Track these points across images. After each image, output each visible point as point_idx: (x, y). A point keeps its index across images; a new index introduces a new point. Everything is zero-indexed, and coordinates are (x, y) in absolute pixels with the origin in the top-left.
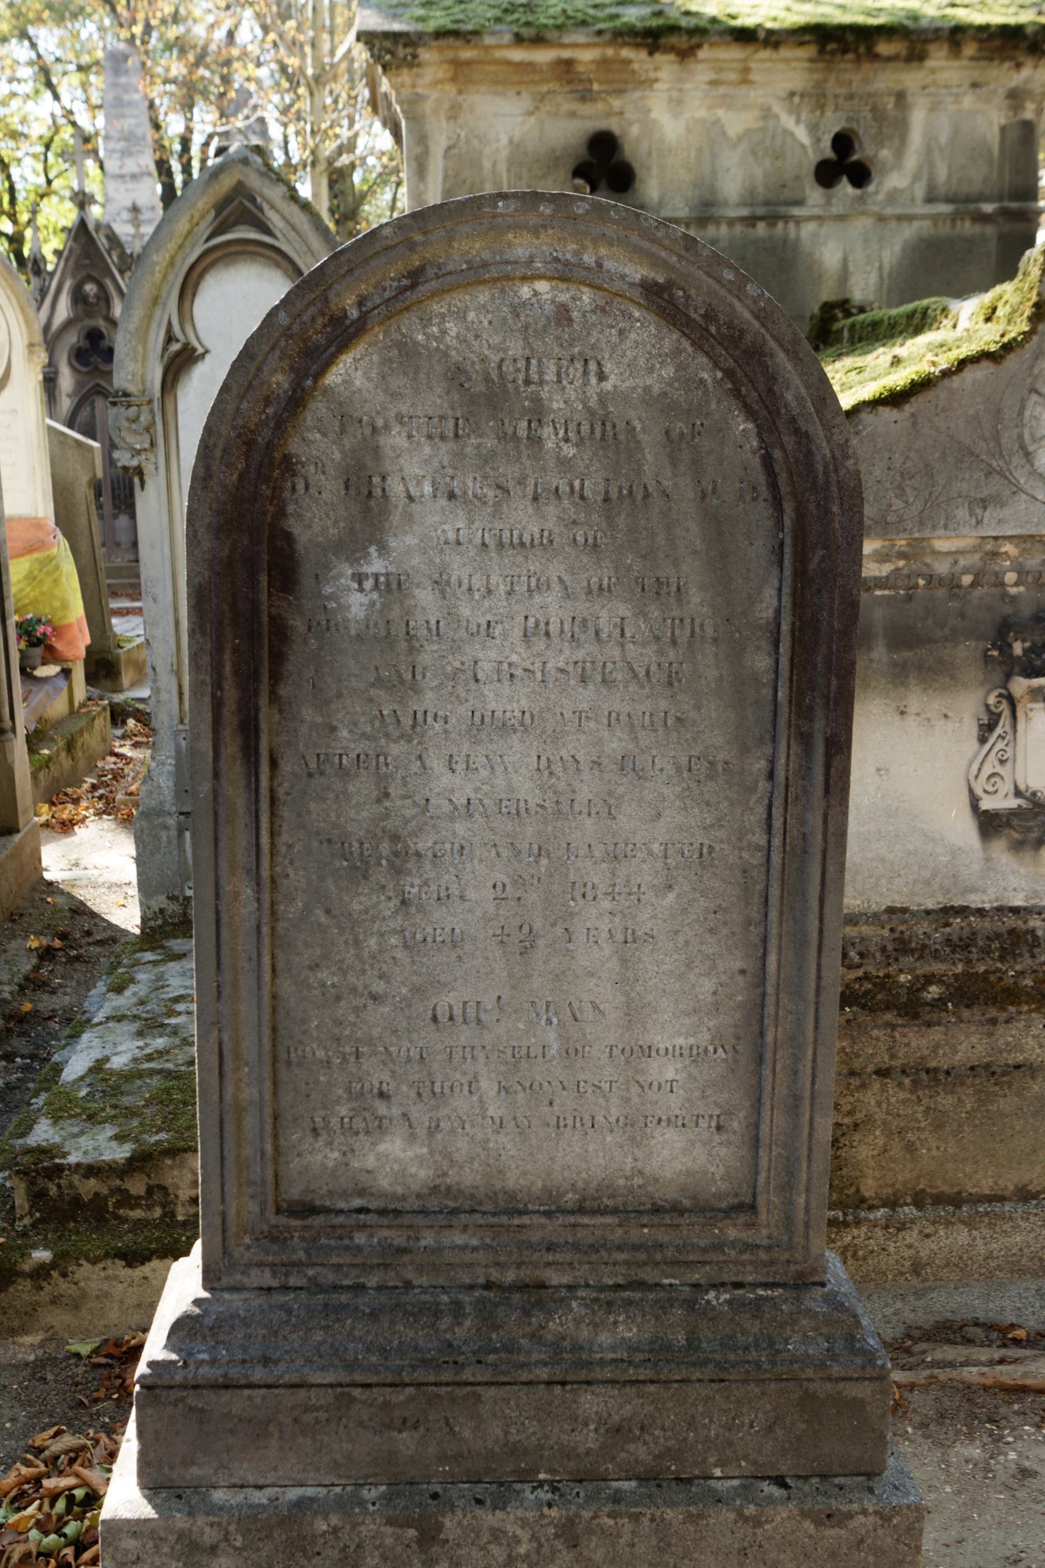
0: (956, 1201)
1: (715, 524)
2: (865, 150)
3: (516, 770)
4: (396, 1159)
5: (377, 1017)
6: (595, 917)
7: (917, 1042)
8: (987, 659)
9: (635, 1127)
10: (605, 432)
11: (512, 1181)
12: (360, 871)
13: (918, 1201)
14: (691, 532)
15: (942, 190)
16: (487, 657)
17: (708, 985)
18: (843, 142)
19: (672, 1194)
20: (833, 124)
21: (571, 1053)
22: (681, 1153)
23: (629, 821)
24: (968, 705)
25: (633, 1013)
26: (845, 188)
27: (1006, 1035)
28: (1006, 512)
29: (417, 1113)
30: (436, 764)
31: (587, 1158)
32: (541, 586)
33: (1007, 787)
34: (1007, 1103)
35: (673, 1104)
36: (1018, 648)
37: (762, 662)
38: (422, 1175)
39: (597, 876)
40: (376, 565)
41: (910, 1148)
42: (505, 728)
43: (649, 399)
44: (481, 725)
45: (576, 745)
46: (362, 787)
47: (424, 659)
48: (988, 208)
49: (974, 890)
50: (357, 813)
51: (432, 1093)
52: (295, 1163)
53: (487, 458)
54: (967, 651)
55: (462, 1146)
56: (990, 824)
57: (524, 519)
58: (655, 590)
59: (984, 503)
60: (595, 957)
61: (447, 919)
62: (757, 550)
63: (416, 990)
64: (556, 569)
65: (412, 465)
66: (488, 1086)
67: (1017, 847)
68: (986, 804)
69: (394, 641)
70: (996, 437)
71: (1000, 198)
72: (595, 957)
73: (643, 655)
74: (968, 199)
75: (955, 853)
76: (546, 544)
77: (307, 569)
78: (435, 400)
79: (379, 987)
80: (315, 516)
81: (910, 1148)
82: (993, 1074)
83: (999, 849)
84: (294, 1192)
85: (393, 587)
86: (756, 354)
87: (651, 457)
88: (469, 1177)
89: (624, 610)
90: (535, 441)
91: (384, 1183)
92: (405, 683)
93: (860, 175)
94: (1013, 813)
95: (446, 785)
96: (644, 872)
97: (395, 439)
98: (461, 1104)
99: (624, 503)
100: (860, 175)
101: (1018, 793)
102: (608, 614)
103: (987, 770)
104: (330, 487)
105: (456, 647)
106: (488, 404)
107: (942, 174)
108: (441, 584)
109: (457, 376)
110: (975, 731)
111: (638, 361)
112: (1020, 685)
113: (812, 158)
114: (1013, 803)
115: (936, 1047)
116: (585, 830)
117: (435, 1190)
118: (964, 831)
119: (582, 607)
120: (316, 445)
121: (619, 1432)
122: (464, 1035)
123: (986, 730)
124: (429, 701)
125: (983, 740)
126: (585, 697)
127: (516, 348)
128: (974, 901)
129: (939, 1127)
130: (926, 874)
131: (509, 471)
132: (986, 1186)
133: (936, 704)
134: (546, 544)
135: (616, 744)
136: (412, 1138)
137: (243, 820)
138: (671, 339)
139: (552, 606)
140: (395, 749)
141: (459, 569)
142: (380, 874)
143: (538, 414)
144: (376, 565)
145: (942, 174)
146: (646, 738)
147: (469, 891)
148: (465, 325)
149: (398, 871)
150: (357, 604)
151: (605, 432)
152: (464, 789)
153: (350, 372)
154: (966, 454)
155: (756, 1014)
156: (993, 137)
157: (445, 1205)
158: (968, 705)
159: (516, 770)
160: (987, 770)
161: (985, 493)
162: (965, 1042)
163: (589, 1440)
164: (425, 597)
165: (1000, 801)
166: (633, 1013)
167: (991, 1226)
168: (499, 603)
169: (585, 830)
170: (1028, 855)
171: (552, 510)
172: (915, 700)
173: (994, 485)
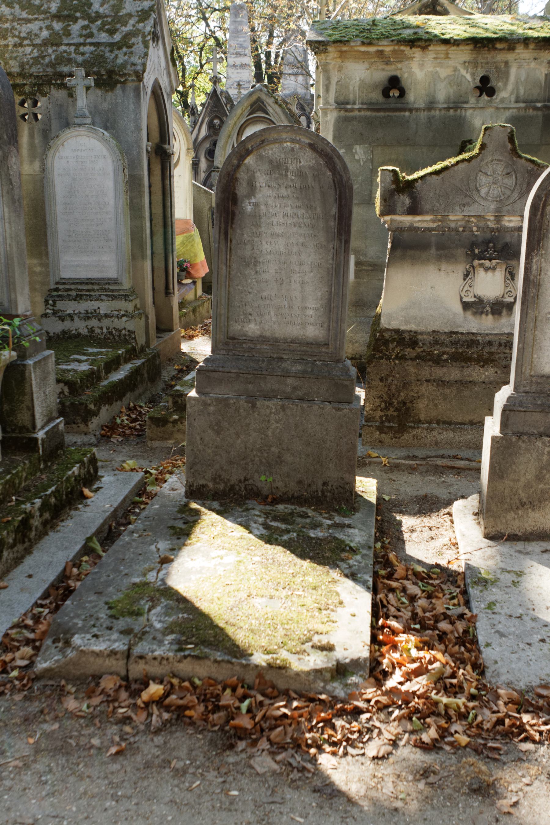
0: (450, 423)
2: (493, 83)
3: (280, 245)
4: (252, 329)
6: (296, 277)
7: (439, 372)
8: (467, 254)
9: (303, 325)
10: (301, 174)
11: (277, 335)
12: (248, 265)
13: (438, 422)
14: (318, 195)
15: (522, 98)
16: (275, 220)
17: (320, 294)
18: (485, 80)
19: (311, 341)
20: (481, 73)
21: (290, 307)
22: (313, 332)
24: (461, 269)
25: (303, 299)
26: (485, 97)
27: (467, 371)
28: (471, 208)
29: (257, 318)
30: (264, 243)
31: (293, 331)
33: (471, 295)
34: (467, 393)
35: (312, 320)
36: (477, 251)
37: (332, 224)
38: (258, 333)
39: (297, 268)
40: (253, 200)
41: (436, 405)
42: (278, 236)
43: (310, 168)
44: (274, 235)
45: (293, 240)
46: (249, 247)
47: (262, 220)
48: (539, 105)
49: (460, 327)
50: (247, 252)
51: (261, 315)
52: (232, 328)
53: (276, 179)
54: (460, 252)
55: (266, 327)
56: (466, 306)
57: (284, 192)
58: (310, 207)
59: (464, 205)
61: (265, 276)
63: (259, 292)
64: (290, 202)
65: (261, 180)
66: (272, 314)
67: (475, 314)
68: (465, 299)
69: (256, 216)
70: (468, 185)
71: (544, 101)
74: (532, 102)
75: (455, 314)
76: (288, 197)
77: (239, 201)
78: (266, 167)
79: (250, 290)
80: (241, 190)
81: (436, 405)
82: (463, 384)
83: (469, 314)
85: (256, 205)
86: (331, 158)
87: (310, 180)
88: (268, 334)
89: (303, 211)
90: (286, 175)
91: (250, 334)
92: (258, 225)
93: (491, 92)
94: (474, 303)
95: (266, 247)
96: (306, 268)
97: (258, 174)
98: (267, 317)
100: (491, 92)
101: (475, 297)
102: (300, 212)
103: (465, 289)
104: (244, 184)
105: (269, 218)
106: (277, 168)
107: (522, 92)
108: (266, 205)
109: (271, 162)
110: (462, 277)
112: (476, 262)
113: (472, 85)
114: (473, 299)
115: (444, 374)
117: (260, 336)
118: (458, 308)
119: (295, 210)
120: (242, 175)
121: (295, 388)
122: (268, 302)
123: (466, 276)
124: (263, 229)
125: (465, 280)
126: (295, 229)
127: (283, 156)
128: (460, 330)
129: (445, 399)
130: (445, 321)
131: (281, 182)
132: (460, 420)
133: (450, 268)
134: (288, 197)
135: (301, 240)
136: (256, 324)
137: (224, 253)
138: (314, 155)
139: (289, 210)
140: (256, 239)
141: (270, 202)
142: (251, 266)
143: (287, 170)
144: (253, 200)
145: (522, 92)
146: (307, 239)
147: (270, 270)
148: (272, 151)
149: (255, 265)
150: (249, 208)
151: (301, 174)
153: (249, 160)
155: (330, 300)
156: (542, 78)
157: (263, 339)
158: (461, 269)
159: (280, 245)
160: (465, 289)
161: (464, 202)
162: (454, 373)
163: (289, 389)
164: (263, 207)
165: (469, 299)
166: (303, 299)
167: (461, 432)
168: (278, 209)
169: (294, 258)
170: (478, 317)
171: (289, 190)
172: (444, 266)
173: (468, 200)
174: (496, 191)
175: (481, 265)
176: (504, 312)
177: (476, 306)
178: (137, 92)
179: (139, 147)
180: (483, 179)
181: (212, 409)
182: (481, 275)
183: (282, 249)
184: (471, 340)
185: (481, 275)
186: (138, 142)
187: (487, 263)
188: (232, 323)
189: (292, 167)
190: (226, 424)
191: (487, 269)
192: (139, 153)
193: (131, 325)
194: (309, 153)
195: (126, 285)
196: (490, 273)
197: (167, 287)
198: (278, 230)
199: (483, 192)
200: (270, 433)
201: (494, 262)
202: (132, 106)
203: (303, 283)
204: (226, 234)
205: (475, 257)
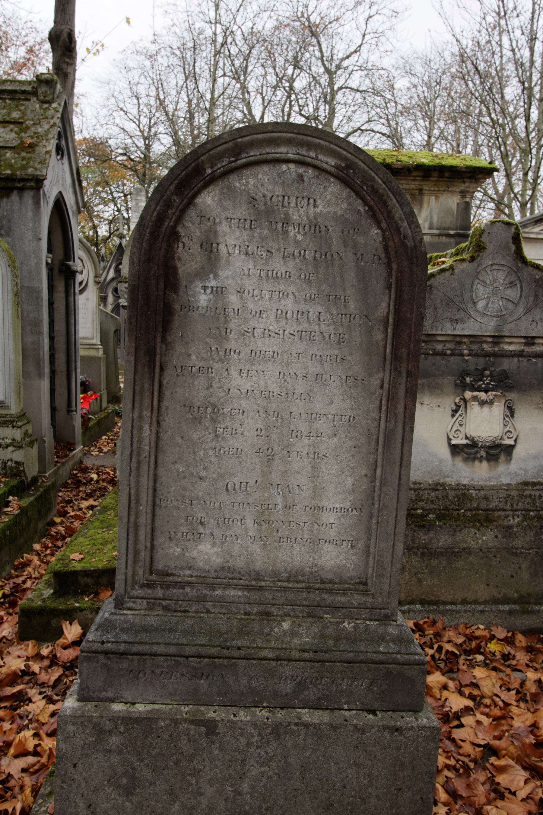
0: (436, 603)
1: (363, 275)
3: (269, 378)
4: (206, 553)
5: (201, 488)
6: (302, 445)
9: (315, 543)
10: (315, 228)
11: (258, 565)
12: (198, 420)
13: (423, 602)
14: (351, 275)
15: (435, 225)
16: (259, 327)
17: (350, 481)
19: (330, 576)
22: (335, 556)
23: (319, 405)
24: (449, 402)
27: (459, 536)
28: (466, 325)
29: (218, 533)
30: (234, 373)
31: (294, 556)
32: (284, 295)
33: (462, 435)
34: (460, 564)
35: (333, 534)
36: (468, 380)
37: (379, 336)
39: (304, 429)
41: (420, 581)
42: (265, 359)
43: (335, 217)
45: (296, 368)
46: (200, 382)
47: (232, 326)
48: (452, 232)
49: (448, 477)
52: (160, 552)
53: (264, 239)
54: (448, 381)
56: (455, 450)
57: (278, 265)
58: (333, 300)
59: (457, 321)
60: (301, 465)
63: (220, 476)
64: (292, 289)
65: (230, 238)
66: (249, 522)
67: (466, 460)
68: (454, 442)
69: (219, 316)
70: (462, 296)
71: (456, 229)
72: (301, 465)
74: (445, 229)
75: (441, 461)
76: (288, 276)
77: (183, 283)
79: (203, 473)
81: (420, 581)
84: (159, 565)
85: (219, 292)
86: (382, 201)
87: (336, 244)
88: (239, 564)
89: (320, 309)
90: (286, 233)
91: (200, 564)
92: (222, 336)
94: (467, 446)
95: (238, 382)
96: (324, 426)
97: (224, 228)
98: (237, 528)
99: (323, 262)
101: (467, 438)
102: (314, 309)
103: (455, 428)
104: (195, 248)
105: (245, 321)
106: (265, 216)
107: (435, 219)
108: (240, 292)
110: (450, 413)
112: (468, 394)
114: (464, 442)
115: (430, 541)
116: (298, 407)
117: (223, 568)
118: (445, 452)
119: (303, 307)
121: (301, 685)
122: (240, 497)
124: (233, 345)
125: (453, 416)
126: (301, 347)
127: (279, 191)
128: (448, 480)
129: (431, 573)
130: (429, 469)
131: (274, 245)
132: (450, 598)
133: (435, 401)
134: (288, 276)
135: (314, 368)
136: (214, 544)
137: (147, 393)
138: (346, 192)
139: (289, 305)
140: (216, 366)
141: (249, 285)
142: (206, 422)
143: (286, 222)
144: (213, 283)
145: (435, 219)
146: (328, 367)
147: (246, 431)
149: (214, 421)
150: (203, 299)
151: (315, 228)
156: (454, 207)
157: (226, 576)
158: (449, 402)
159: (269, 378)
160: (455, 428)
161: (457, 318)
163: (288, 687)
164: (233, 299)
166: (316, 492)
167: (451, 615)
168: (266, 303)
169: (298, 407)
170: (470, 464)
171: (291, 263)
173: (461, 314)
174: (496, 305)
175: (475, 398)
176: (502, 457)
177: (468, 450)
178: (37, 203)
179: (39, 258)
180: (481, 291)
181: (114, 740)
182: (475, 409)
183: (274, 387)
184: (463, 493)
185: (475, 409)
186: (37, 252)
187: (483, 396)
188: (160, 540)
189: (299, 213)
190: (147, 774)
191: (482, 403)
192: (38, 264)
193: (18, 456)
194: (334, 188)
195: (14, 409)
196: (486, 409)
197: (69, 405)
199: (481, 305)
200: (245, 787)
201: (491, 394)
202: (30, 214)
203: (317, 457)
204: (151, 353)
205: (463, 387)
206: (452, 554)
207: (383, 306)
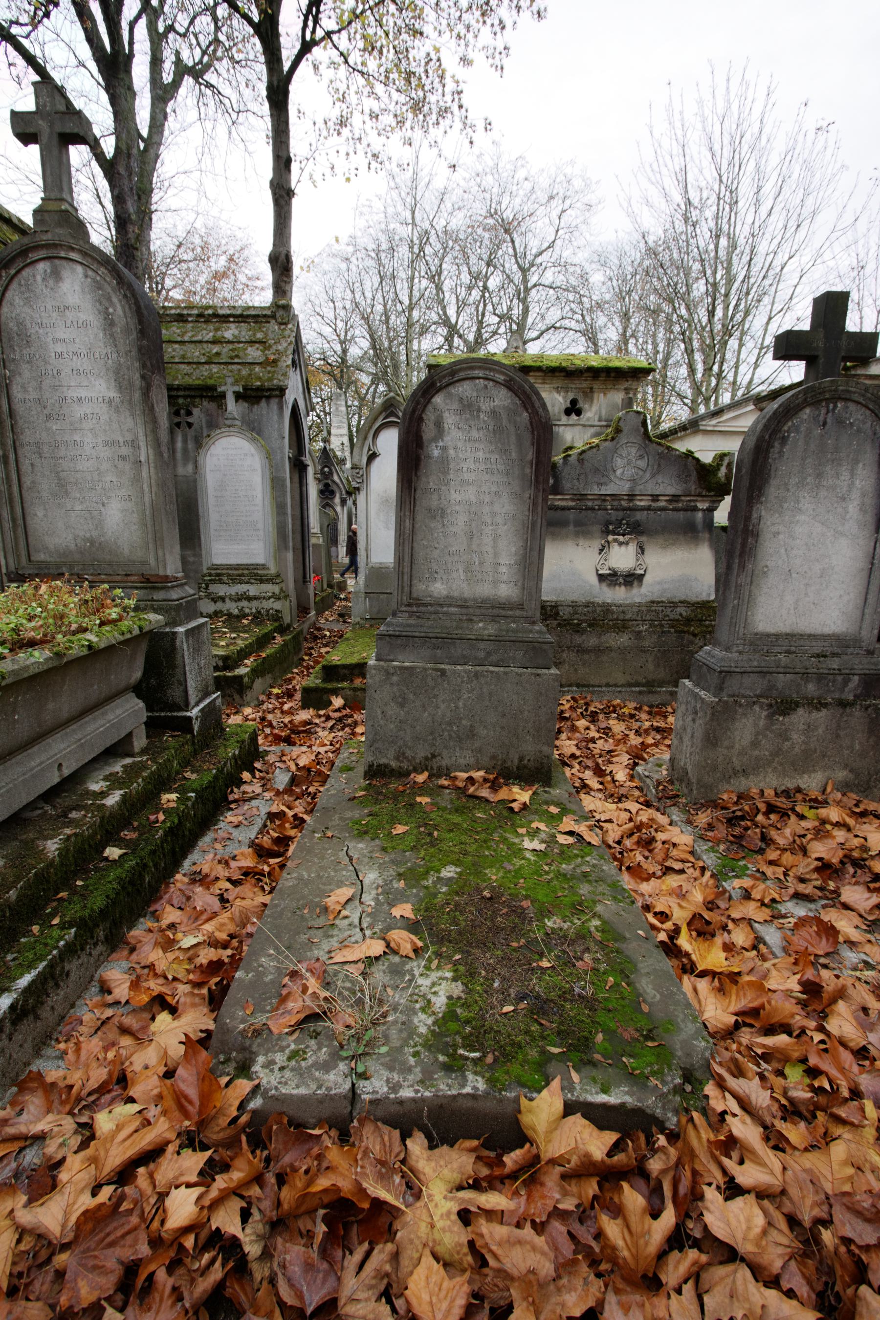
0: (588, 686)
1: (519, 438)
2: (580, 404)
3: (471, 494)
4: (439, 589)
5: (436, 553)
6: (488, 530)
7: (578, 639)
9: (495, 583)
10: (494, 413)
11: (466, 595)
13: (578, 686)
14: (513, 439)
16: (465, 466)
18: (574, 402)
20: (571, 396)
21: (481, 563)
23: (497, 508)
24: (597, 544)
25: (496, 555)
26: (574, 417)
31: (484, 590)
32: (478, 450)
34: (604, 658)
35: (505, 578)
37: (528, 471)
38: (445, 593)
39: (489, 521)
40: (441, 444)
42: (468, 484)
43: (504, 407)
44: (463, 482)
45: (485, 488)
46: (435, 497)
50: (434, 504)
51: (447, 571)
54: (597, 528)
55: (454, 587)
56: (602, 578)
57: (475, 434)
58: (504, 452)
60: (488, 540)
61: (453, 529)
62: (527, 443)
65: (450, 420)
67: (609, 585)
69: (444, 461)
72: (488, 540)
73: (501, 467)
76: (480, 439)
78: (456, 406)
80: (428, 430)
83: (604, 585)
84: (415, 595)
85: (444, 449)
86: (529, 398)
87: (505, 422)
88: (456, 594)
92: (446, 472)
93: (579, 413)
95: (454, 496)
96: (499, 519)
97: (446, 415)
98: (455, 575)
99: (498, 431)
100: (579, 413)
104: (431, 425)
106: (468, 407)
107: (604, 413)
109: (461, 399)
111: (502, 398)
112: (610, 538)
113: (564, 407)
116: (486, 509)
118: (594, 580)
120: (429, 416)
123: (601, 550)
124: (451, 476)
126: (487, 477)
128: (597, 600)
133: (587, 543)
134: (480, 439)
135: (494, 489)
138: (510, 394)
139: (481, 455)
141: (460, 445)
143: (479, 410)
144: (441, 444)
145: (604, 413)
147: (459, 522)
148: (465, 389)
150: (436, 453)
151: (494, 413)
152: (459, 498)
153: (438, 399)
154: (597, 470)
155: (524, 556)
156: (620, 402)
157: (449, 601)
158: (597, 544)
159: (471, 494)
162: (592, 641)
163: (482, 655)
164: (451, 452)
165: (605, 571)
166: (496, 555)
169: (486, 509)
172: (581, 542)
174: (630, 472)
175: (615, 540)
176: (636, 583)
177: (610, 578)
178: (281, 408)
179: (283, 452)
180: (619, 462)
181: (395, 679)
182: (615, 549)
183: (473, 499)
184: (607, 608)
185: (615, 549)
186: (281, 448)
187: (621, 538)
188: (415, 582)
189: (485, 405)
190: (411, 696)
191: (621, 544)
192: (282, 458)
193: (277, 605)
194: (504, 392)
195: (273, 571)
196: (623, 548)
197: (304, 577)
198: (467, 476)
199: (619, 472)
200: (461, 704)
201: (627, 537)
202: (276, 417)
203: (496, 536)
204: (410, 482)
205: (608, 532)
206: (599, 651)
207: (530, 455)
